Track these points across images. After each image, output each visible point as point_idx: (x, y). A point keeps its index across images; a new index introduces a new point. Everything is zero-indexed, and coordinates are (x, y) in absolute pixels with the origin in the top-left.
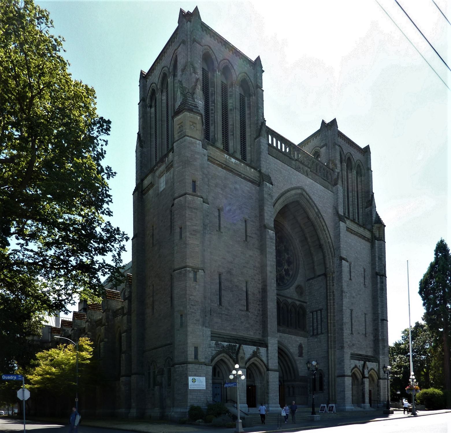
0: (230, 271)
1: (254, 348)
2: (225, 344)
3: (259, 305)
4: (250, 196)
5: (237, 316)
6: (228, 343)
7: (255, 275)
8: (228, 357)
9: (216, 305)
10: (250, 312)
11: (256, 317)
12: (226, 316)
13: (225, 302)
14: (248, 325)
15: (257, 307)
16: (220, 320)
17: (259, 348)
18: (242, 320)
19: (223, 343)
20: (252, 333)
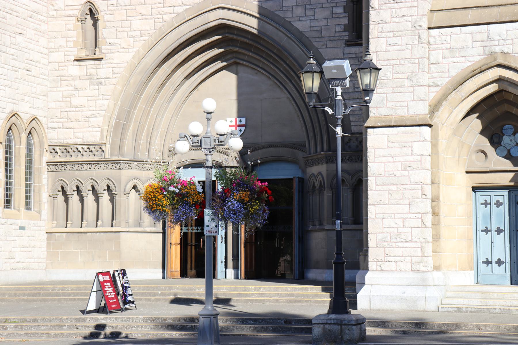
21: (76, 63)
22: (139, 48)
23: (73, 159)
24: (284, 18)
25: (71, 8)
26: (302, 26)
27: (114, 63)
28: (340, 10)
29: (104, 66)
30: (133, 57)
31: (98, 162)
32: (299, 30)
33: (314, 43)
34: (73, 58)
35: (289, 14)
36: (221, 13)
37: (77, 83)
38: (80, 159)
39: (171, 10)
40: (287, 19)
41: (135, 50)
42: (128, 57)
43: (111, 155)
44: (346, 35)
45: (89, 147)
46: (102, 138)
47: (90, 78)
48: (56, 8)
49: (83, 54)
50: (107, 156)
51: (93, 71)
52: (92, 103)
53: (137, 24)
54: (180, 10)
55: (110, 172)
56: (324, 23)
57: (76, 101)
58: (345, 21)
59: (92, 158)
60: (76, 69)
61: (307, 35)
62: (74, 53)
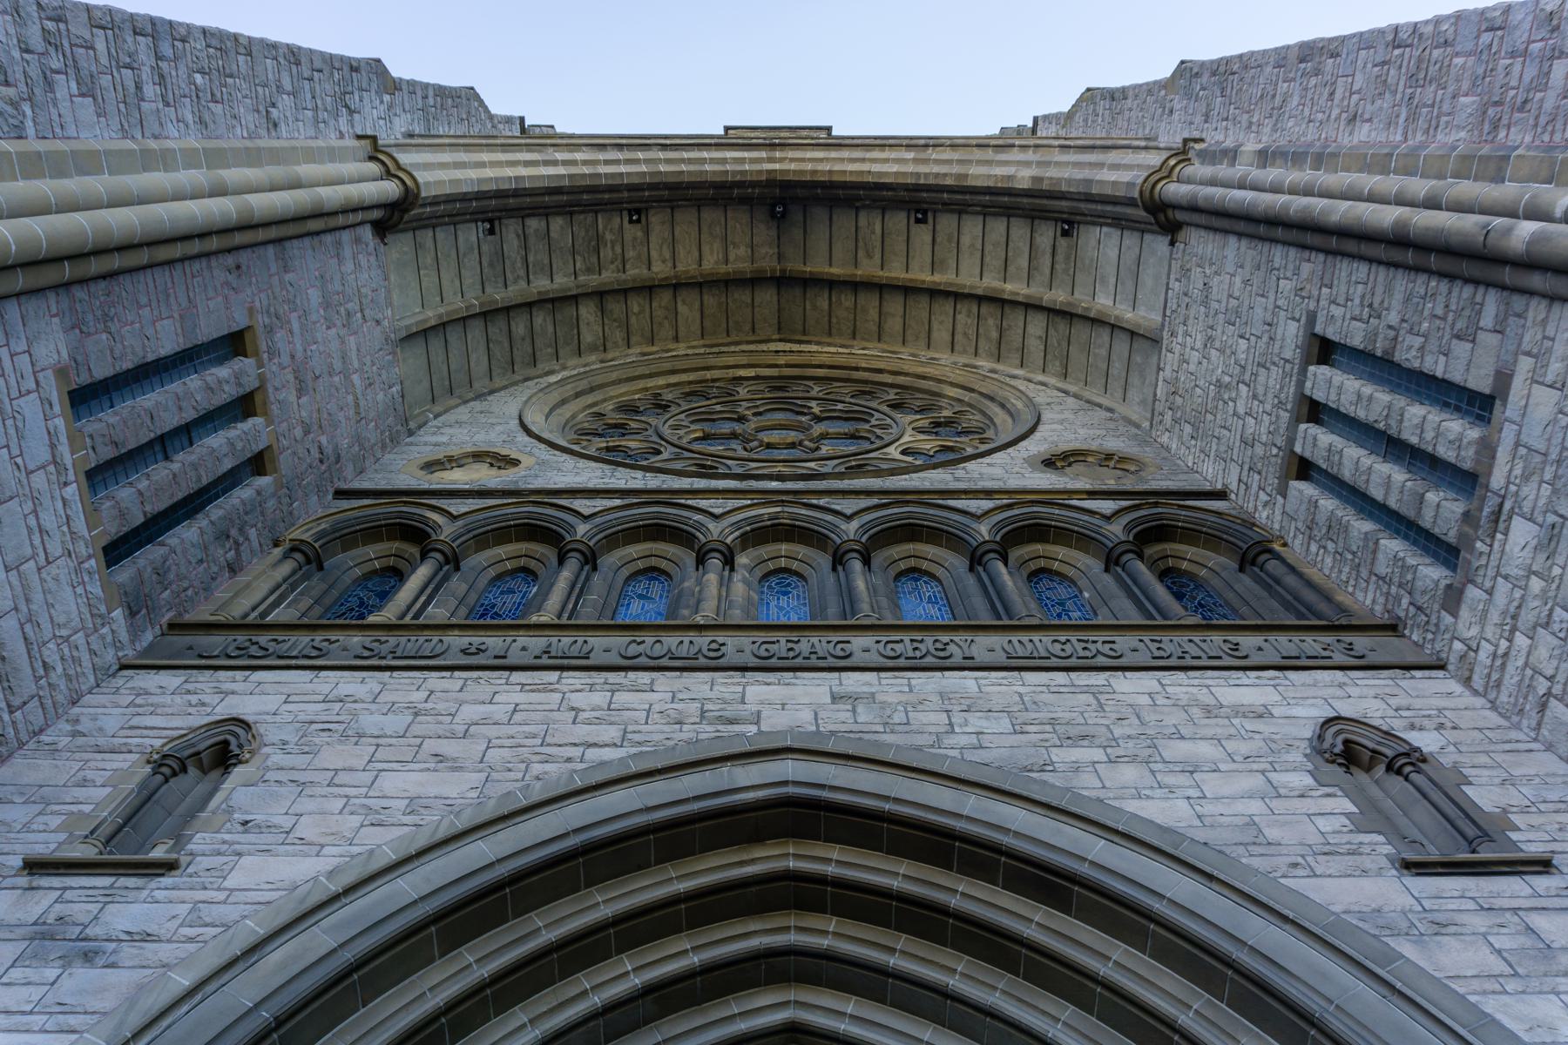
21: (23, 881)
22: (379, 846)
24: (1068, 789)
25: (146, 732)
27: (219, 889)
29: (159, 894)
30: (330, 874)
32: (1152, 822)
33: (1244, 860)
34: (17, 862)
36: (788, 769)
39: (575, 752)
40: (1085, 793)
41: (355, 850)
48: (79, 728)
51: (80, 911)
61: (1201, 835)
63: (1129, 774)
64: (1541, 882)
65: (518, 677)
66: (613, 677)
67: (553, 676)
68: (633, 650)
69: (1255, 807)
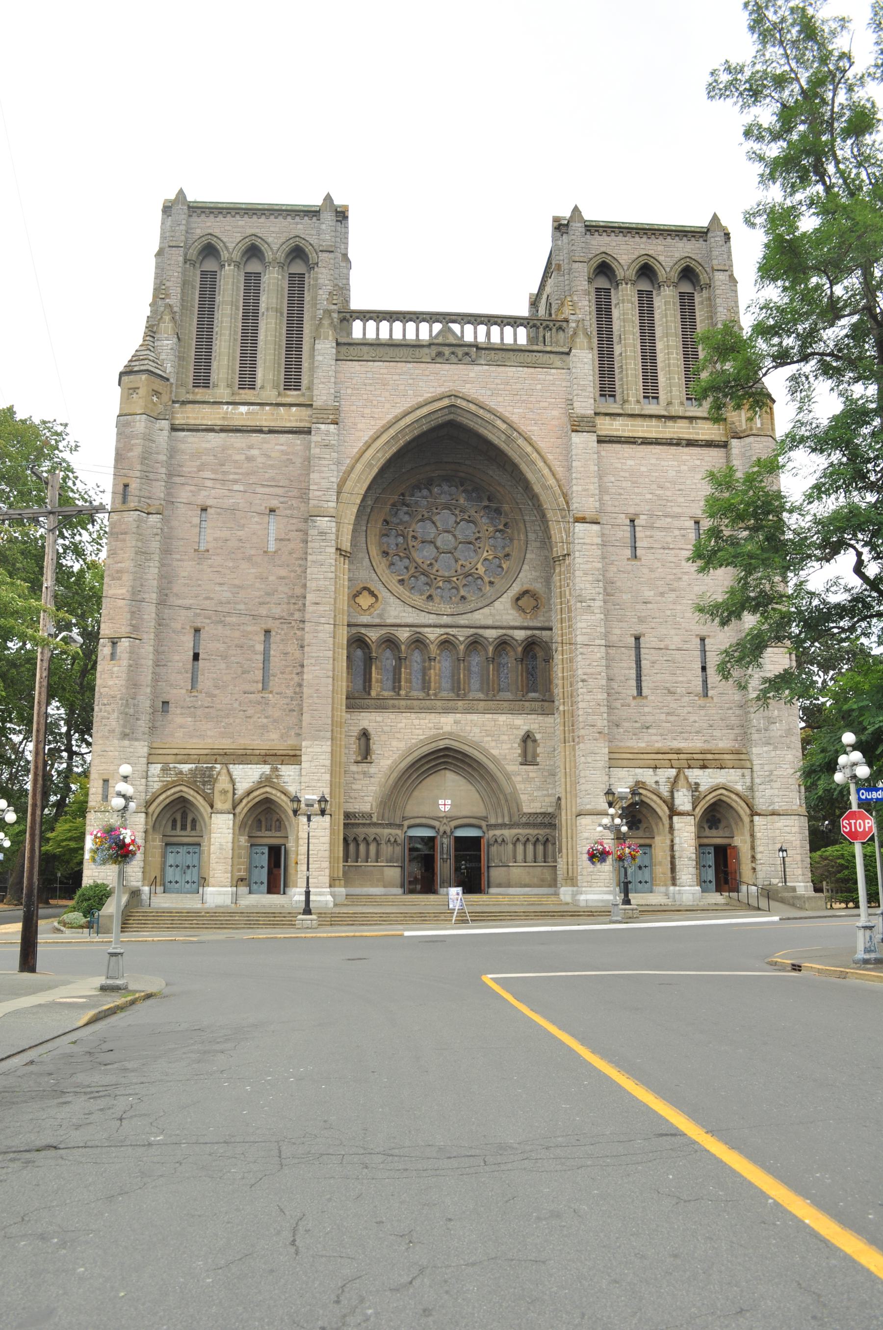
0: (223, 619)
1: (267, 769)
2: (186, 768)
3: (298, 674)
4: (288, 459)
5: (236, 705)
6: (194, 766)
7: (292, 614)
8: (192, 792)
9: (184, 691)
10: (271, 692)
11: (288, 701)
12: (207, 710)
13: (205, 682)
14: (265, 721)
15: (292, 679)
16: (190, 719)
17: (279, 766)
18: (250, 712)
19: (182, 766)
20: (274, 736)
23: (353, 821)
26: (495, 752)
28: (516, 745)
31: (369, 824)
35: (487, 745)
36: (447, 742)
37: (356, 776)
38: (357, 821)
42: (389, 762)
43: (378, 819)
44: (520, 760)
45: (364, 815)
46: (371, 809)
47: (364, 773)
49: (359, 759)
50: (375, 820)
52: (364, 788)
53: (395, 743)
54: (422, 737)
55: (379, 830)
56: (507, 751)
57: (354, 787)
58: (519, 751)
59: (364, 821)
60: (354, 768)
62: (353, 758)
63: (493, 744)
64: (535, 767)
65: (404, 714)
66: (419, 715)
67: (409, 714)
68: (422, 706)
69: (507, 751)
